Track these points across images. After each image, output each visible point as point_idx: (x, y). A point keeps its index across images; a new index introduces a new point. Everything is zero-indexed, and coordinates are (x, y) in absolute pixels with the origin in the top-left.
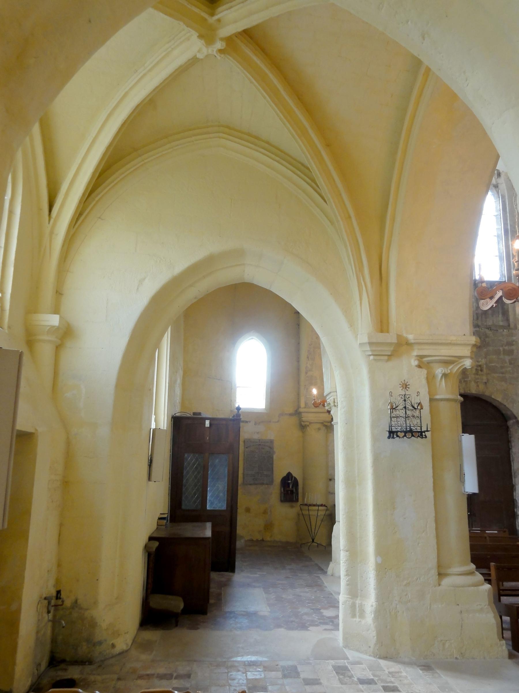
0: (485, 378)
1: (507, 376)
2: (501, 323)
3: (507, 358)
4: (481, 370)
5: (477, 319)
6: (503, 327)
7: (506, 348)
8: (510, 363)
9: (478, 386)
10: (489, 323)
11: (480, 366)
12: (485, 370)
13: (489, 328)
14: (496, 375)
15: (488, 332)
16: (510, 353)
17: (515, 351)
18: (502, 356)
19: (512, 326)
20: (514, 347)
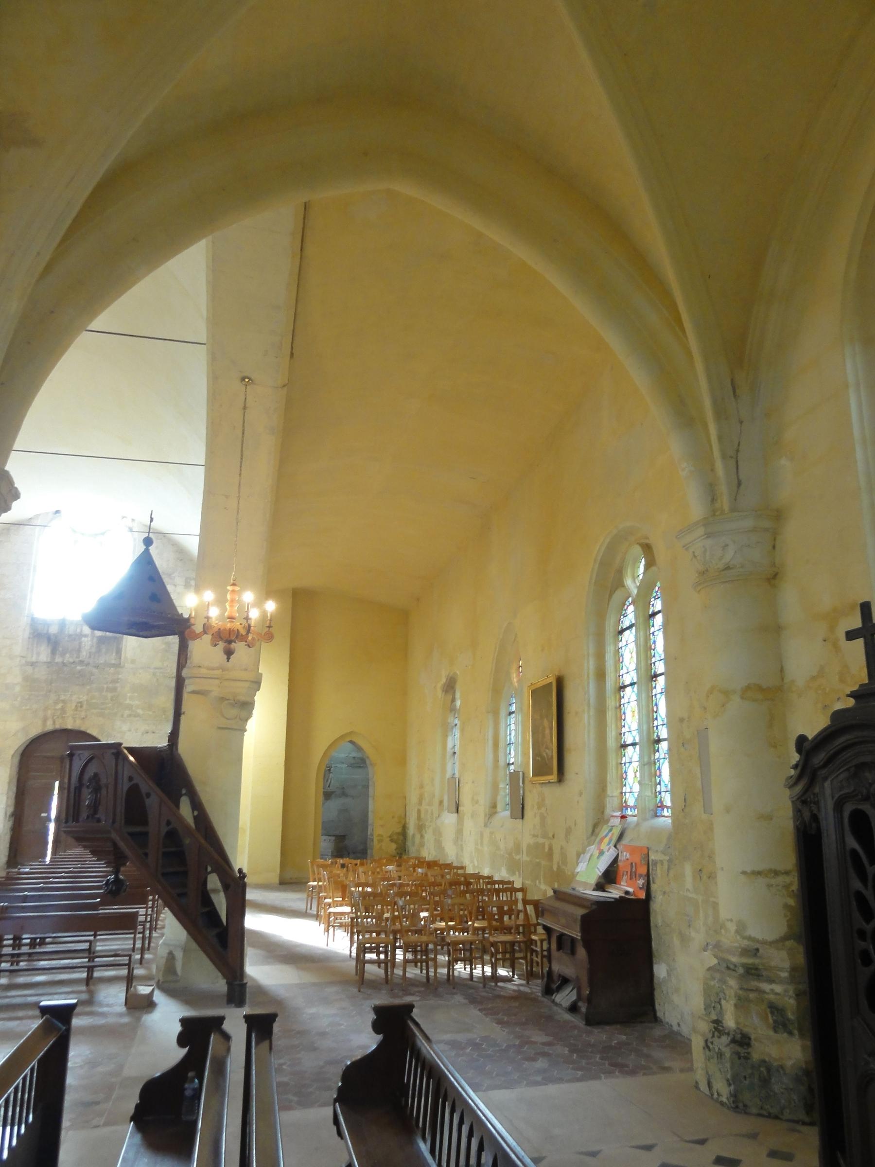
0: (83, 714)
1: (107, 712)
2: (113, 662)
3: (109, 695)
4: (81, 706)
5: (90, 657)
6: (113, 665)
7: (110, 685)
8: (112, 700)
9: (75, 721)
10: (102, 660)
11: (80, 702)
12: (84, 707)
13: (97, 667)
14: (95, 711)
15: (95, 671)
16: (114, 690)
17: (119, 689)
18: (104, 694)
19: (122, 664)
20: (118, 685)
